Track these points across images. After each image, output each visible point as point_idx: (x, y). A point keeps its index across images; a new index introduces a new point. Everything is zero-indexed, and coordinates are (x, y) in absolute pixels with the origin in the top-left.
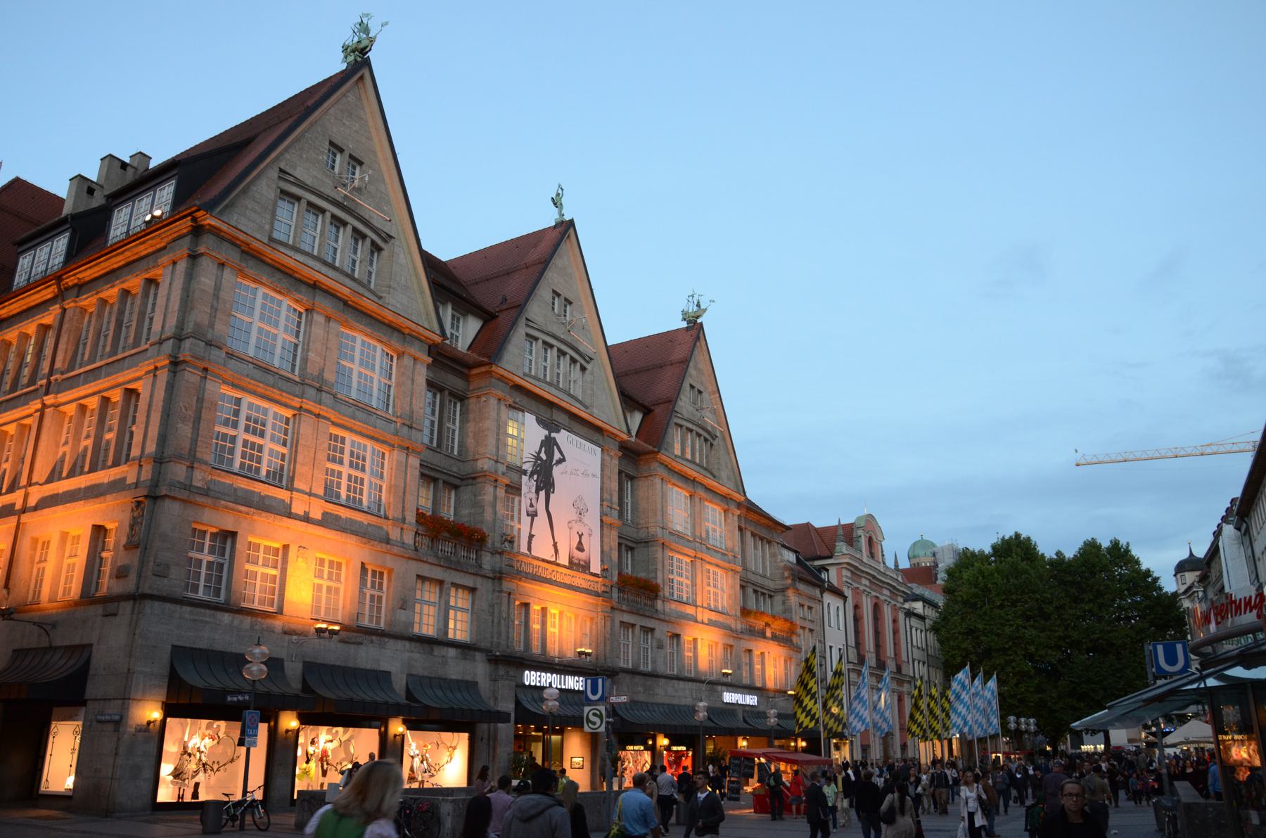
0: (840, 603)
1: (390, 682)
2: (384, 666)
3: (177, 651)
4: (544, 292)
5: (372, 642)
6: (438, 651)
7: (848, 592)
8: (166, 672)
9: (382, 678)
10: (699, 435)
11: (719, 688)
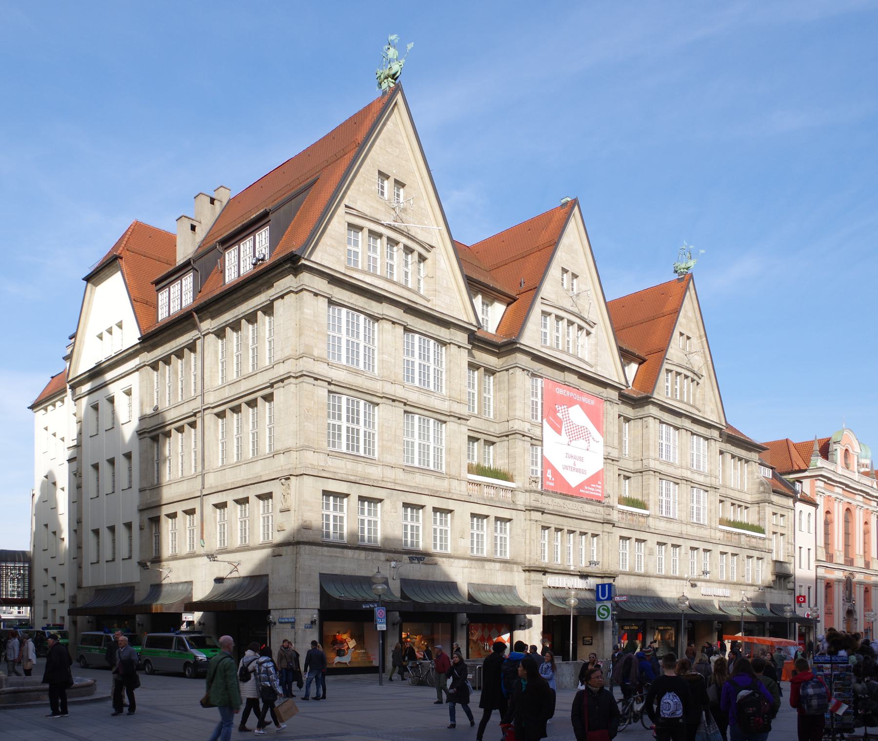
0: (812, 509)
3: (322, 576)
4: (554, 272)
6: (488, 565)
7: (819, 500)
8: (318, 590)
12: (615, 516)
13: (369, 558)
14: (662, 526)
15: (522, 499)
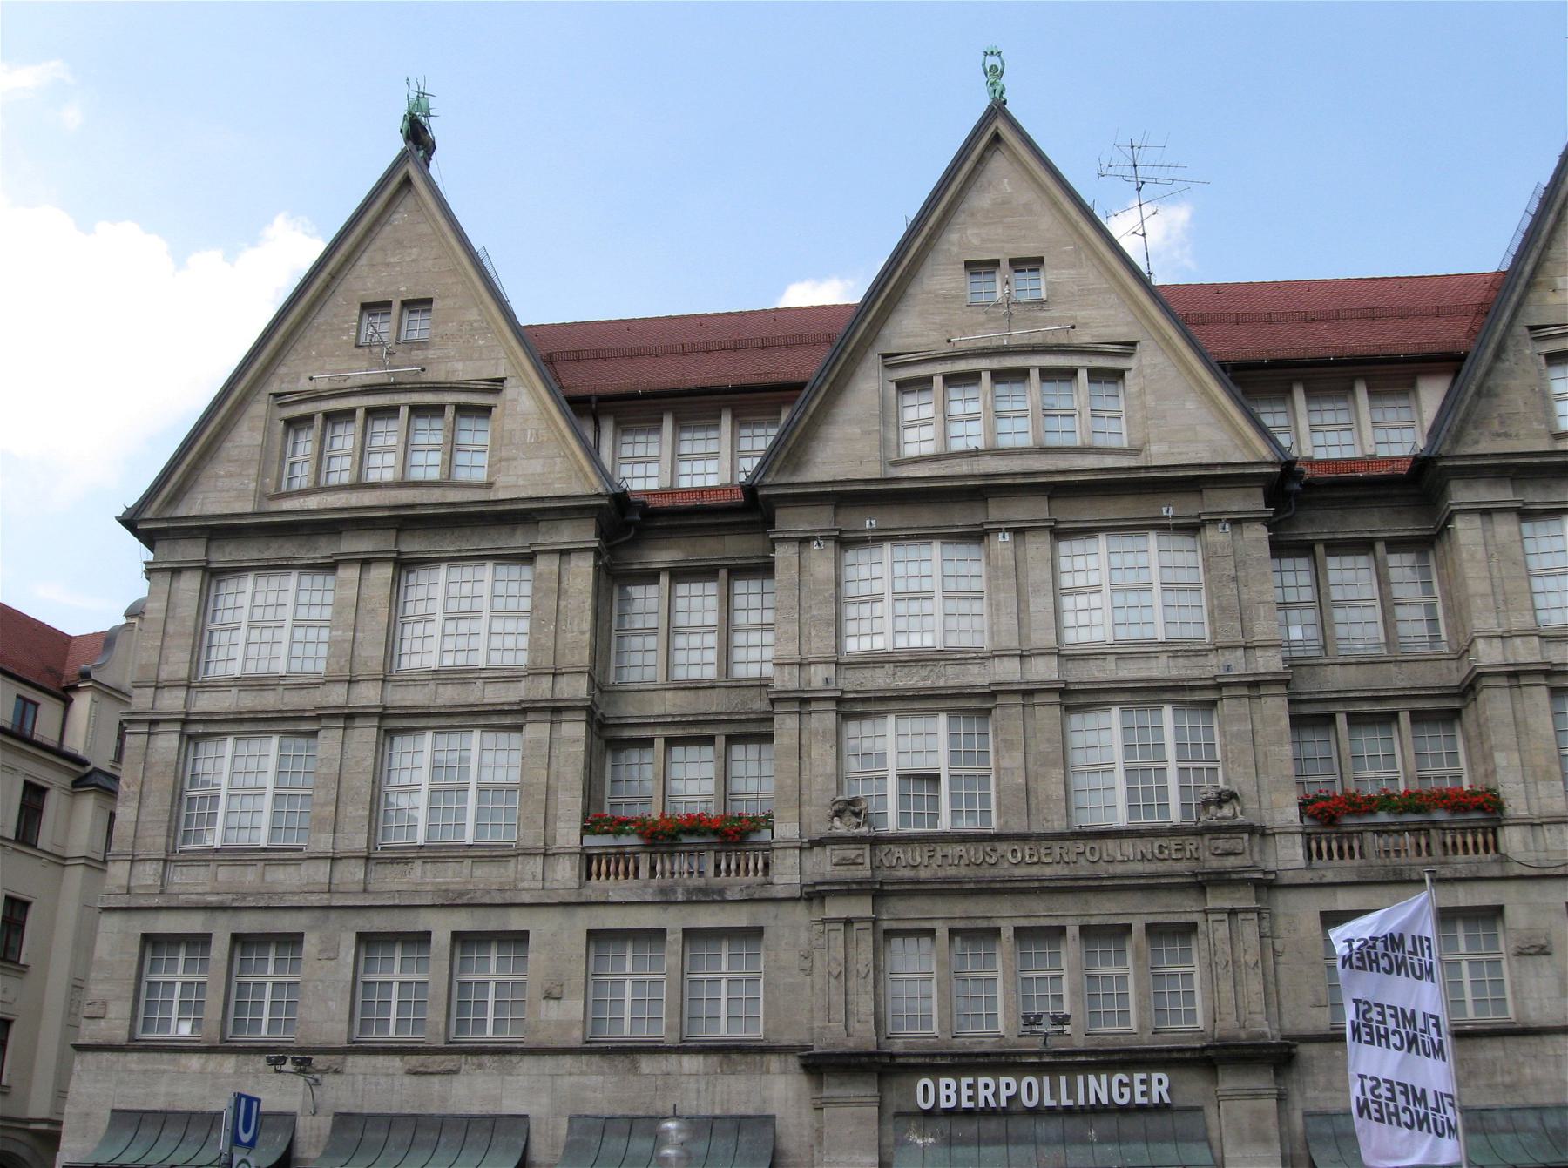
2: (510, 1106)
5: (480, 1066)
6: (647, 1064)
15: (788, 873)
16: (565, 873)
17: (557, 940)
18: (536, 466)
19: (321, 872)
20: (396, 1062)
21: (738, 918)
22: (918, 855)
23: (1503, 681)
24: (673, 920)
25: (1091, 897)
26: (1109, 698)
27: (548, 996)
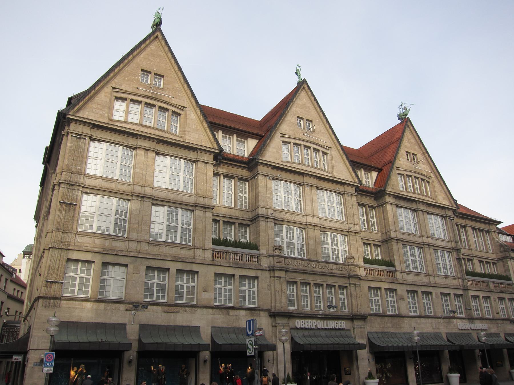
1: (199, 332)
2: (195, 323)
5: (186, 311)
6: (232, 312)
9: (196, 329)
10: (416, 178)
11: (455, 321)
12: (362, 272)
13: (108, 308)
14: (411, 278)
15: (265, 262)
16: (208, 255)
17: (207, 273)
18: (196, 136)
19: (133, 246)
20: (159, 308)
21: (252, 273)
22: (293, 262)
23: (395, 241)
24: (238, 272)
25: (328, 277)
26: (327, 230)
27: (205, 291)
